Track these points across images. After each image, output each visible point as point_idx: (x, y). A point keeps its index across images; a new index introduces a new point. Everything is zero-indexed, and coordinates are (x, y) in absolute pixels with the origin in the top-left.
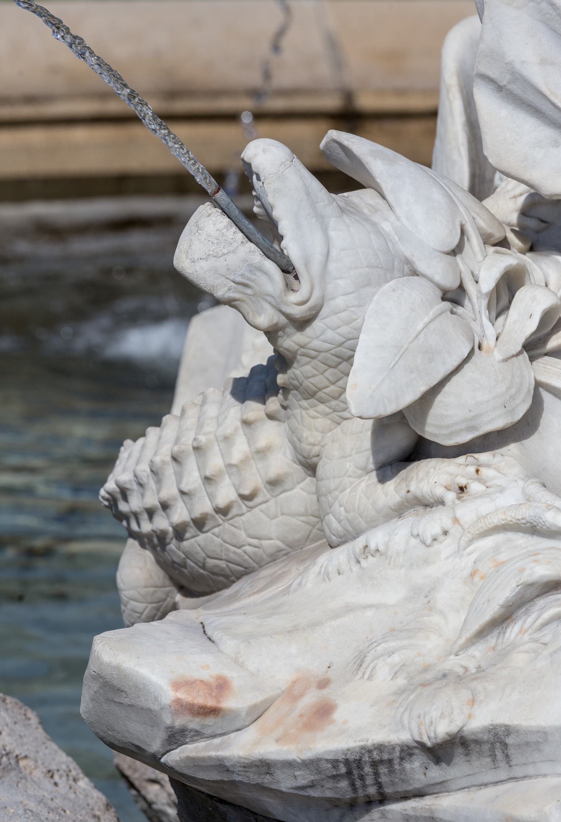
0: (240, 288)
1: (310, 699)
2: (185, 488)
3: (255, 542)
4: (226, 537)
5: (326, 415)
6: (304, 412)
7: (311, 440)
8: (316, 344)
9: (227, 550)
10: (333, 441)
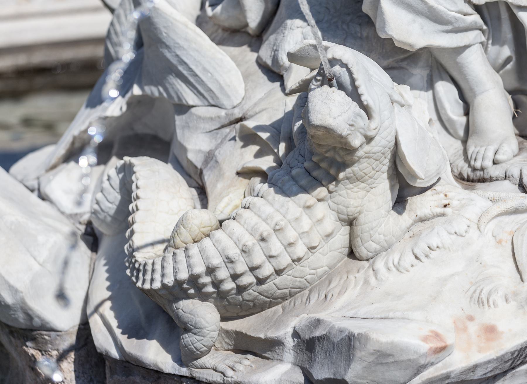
0: (350, 127)
1: (473, 328)
2: (273, 253)
3: (314, 271)
4: (297, 274)
5: (363, 189)
6: (349, 191)
7: (356, 205)
8: (376, 149)
9: (296, 281)
10: (369, 201)
